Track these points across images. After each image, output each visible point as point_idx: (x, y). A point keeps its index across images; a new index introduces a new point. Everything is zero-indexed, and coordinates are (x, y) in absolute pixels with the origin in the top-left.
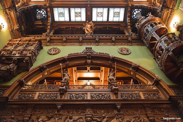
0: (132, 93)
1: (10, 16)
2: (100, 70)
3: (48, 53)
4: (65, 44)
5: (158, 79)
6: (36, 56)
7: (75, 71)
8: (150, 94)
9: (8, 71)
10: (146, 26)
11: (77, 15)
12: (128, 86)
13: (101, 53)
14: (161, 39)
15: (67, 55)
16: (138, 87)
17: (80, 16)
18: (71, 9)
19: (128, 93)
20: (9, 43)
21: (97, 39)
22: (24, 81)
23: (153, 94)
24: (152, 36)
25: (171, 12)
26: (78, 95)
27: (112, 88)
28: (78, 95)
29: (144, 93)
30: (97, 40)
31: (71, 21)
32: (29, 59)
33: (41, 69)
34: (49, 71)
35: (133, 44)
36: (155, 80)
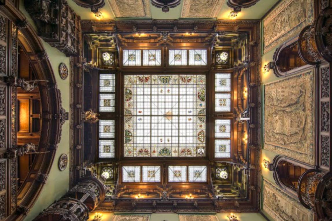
0: (5, 178)
1: (108, 26)
2: (33, 131)
3: (61, 63)
4: (72, 85)
5: (26, 211)
6: (58, 48)
7: (32, 97)
8: (3, 204)
9: (40, 11)
10: (95, 184)
11: (107, 101)
12: (16, 172)
13: (61, 133)
14: (82, 204)
15: (58, 88)
16: (14, 186)
17: (105, 105)
18: (114, 95)
19: (4, 173)
20: (76, 16)
21: (78, 127)
22: (25, 27)
23: (3, 209)
24: (84, 193)
25: (111, 210)
26: (3, 102)
27: (14, 149)
28: (3, 102)
29: (5, 196)
30: (77, 126)
31: (100, 95)
32: (56, 40)
33: (40, 52)
34: (36, 63)
35: (72, 173)
36: (26, 207)
